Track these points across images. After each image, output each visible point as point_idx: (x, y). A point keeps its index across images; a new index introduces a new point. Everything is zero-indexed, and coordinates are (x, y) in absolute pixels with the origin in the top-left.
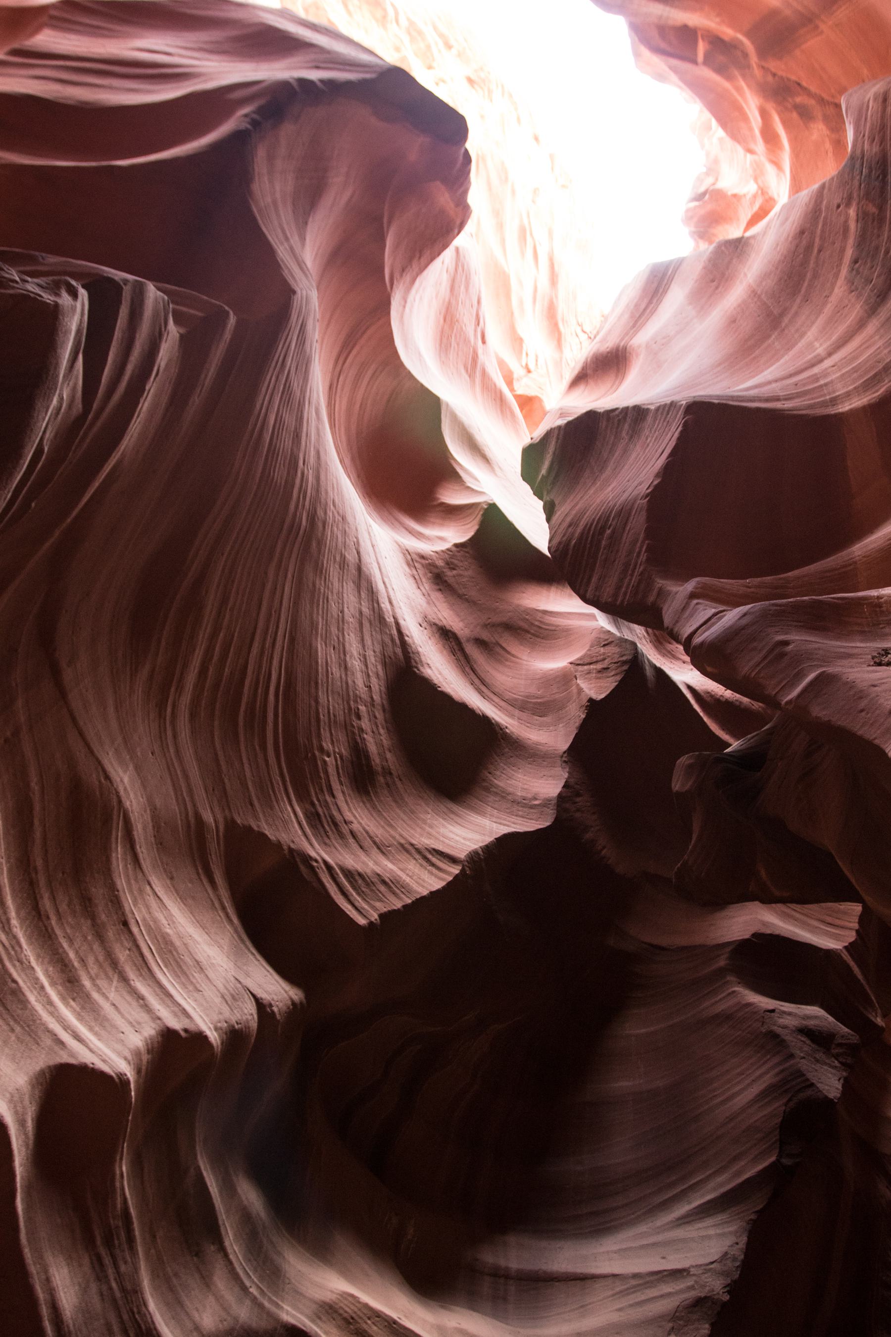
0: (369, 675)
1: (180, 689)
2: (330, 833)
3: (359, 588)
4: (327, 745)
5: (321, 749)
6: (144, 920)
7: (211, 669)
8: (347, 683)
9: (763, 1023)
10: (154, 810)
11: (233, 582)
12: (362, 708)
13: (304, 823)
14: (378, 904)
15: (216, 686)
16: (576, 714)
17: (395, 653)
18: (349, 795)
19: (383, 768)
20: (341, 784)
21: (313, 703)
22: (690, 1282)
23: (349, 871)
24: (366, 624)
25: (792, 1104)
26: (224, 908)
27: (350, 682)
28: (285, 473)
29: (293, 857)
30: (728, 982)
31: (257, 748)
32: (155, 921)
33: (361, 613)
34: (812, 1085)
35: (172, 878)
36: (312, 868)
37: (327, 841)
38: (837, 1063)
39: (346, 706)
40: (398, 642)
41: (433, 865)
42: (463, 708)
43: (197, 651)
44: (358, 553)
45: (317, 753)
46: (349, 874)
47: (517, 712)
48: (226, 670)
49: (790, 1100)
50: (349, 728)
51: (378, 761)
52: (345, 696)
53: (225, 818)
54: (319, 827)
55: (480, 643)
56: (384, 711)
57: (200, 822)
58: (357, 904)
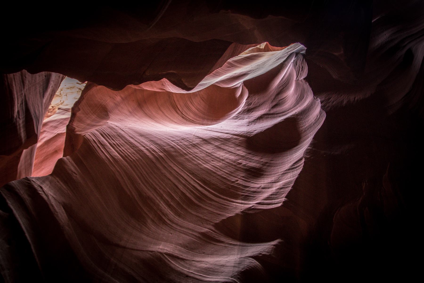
0: (235, 153)
1: (165, 215)
2: (254, 195)
3: (210, 143)
4: (234, 179)
5: (233, 182)
6: (195, 271)
7: (172, 203)
8: (227, 162)
10: (181, 245)
11: (152, 184)
12: (240, 161)
13: (243, 202)
14: (283, 195)
15: (178, 204)
16: (307, 86)
17: (240, 140)
18: (256, 181)
19: (262, 164)
20: (249, 182)
21: (218, 177)
23: (267, 197)
24: (222, 146)
26: (231, 244)
27: (228, 161)
28: (138, 155)
29: (244, 212)
31: (210, 202)
32: (199, 267)
33: (216, 146)
35: (204, 253)
36: (253, 209)
37: (254, 198)
39: (233, 166)
40: (238, 137)
41: (296, 167)
42: (276, 126)
43: (161, 205)
44: (200, 138)
45: (232, 184)
46: (268, 198)
47: (298, 106)
48: (177, 199)
50: (239, 169)
51: (258, 165)
52: (229, 165)
53: (212, 225)
54: (248, 197)
55: (274, 107)
56: (250, 153)
57: (203, 234)
58: (275, 202)
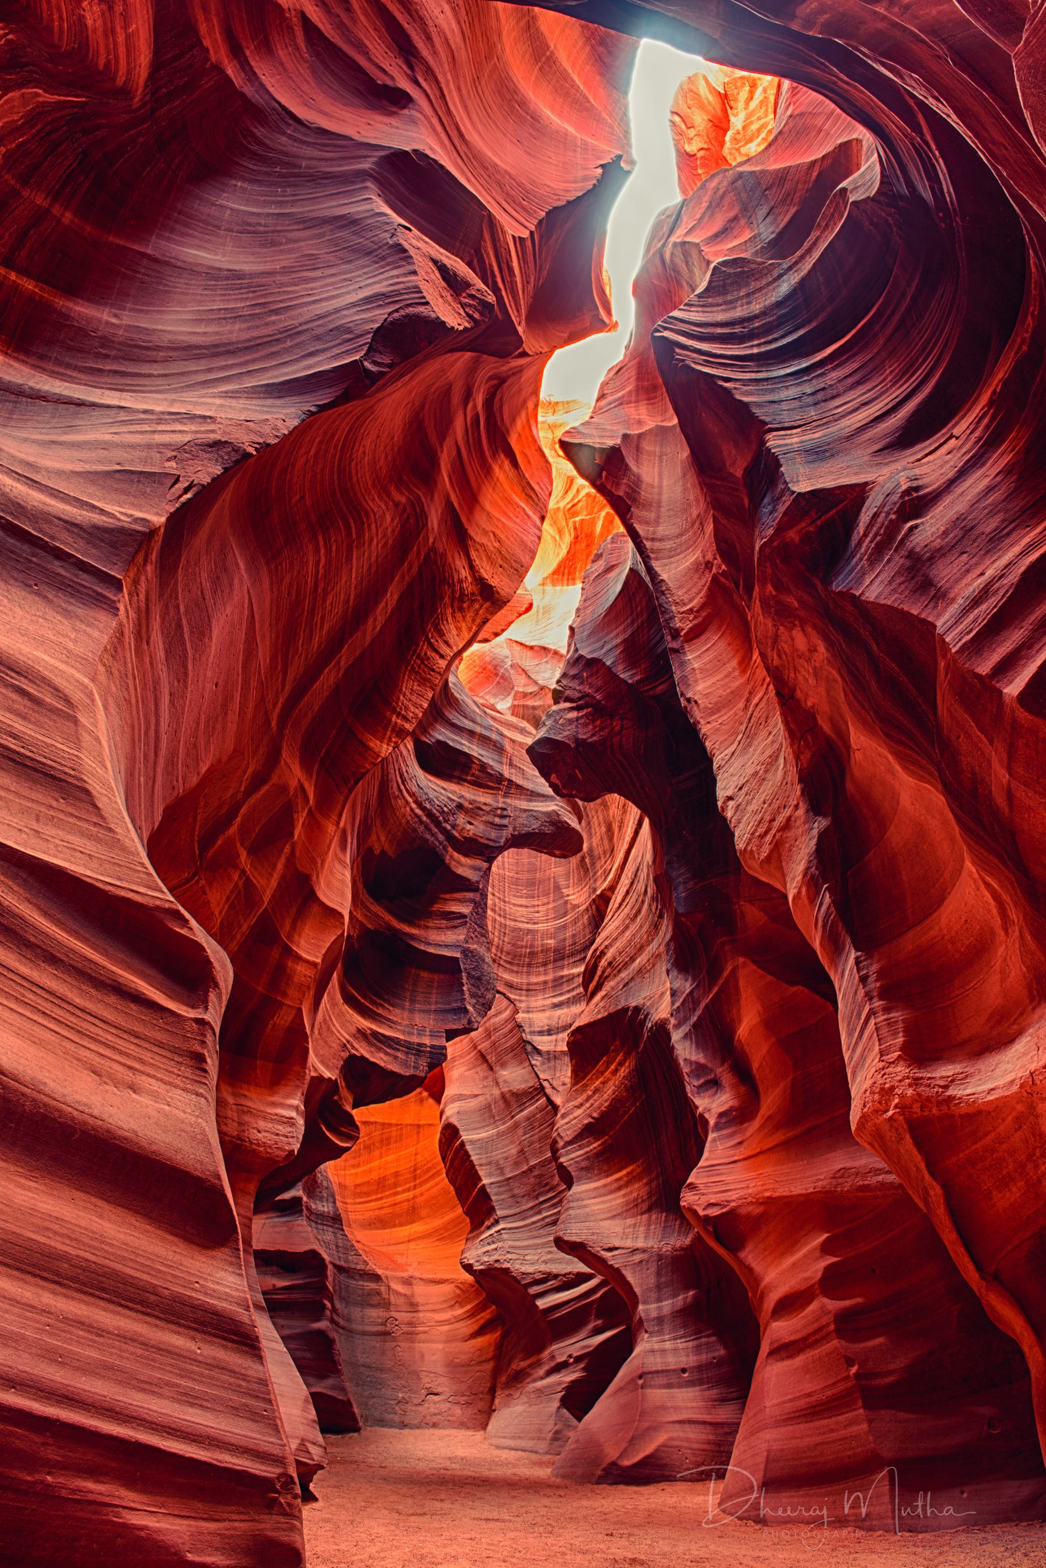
9: (393, 235)
22: (212, 427)
25: (396, 315)
30: (366, 188)
34: (427, 303)
38: (462, 312)
49: (397, 311)
